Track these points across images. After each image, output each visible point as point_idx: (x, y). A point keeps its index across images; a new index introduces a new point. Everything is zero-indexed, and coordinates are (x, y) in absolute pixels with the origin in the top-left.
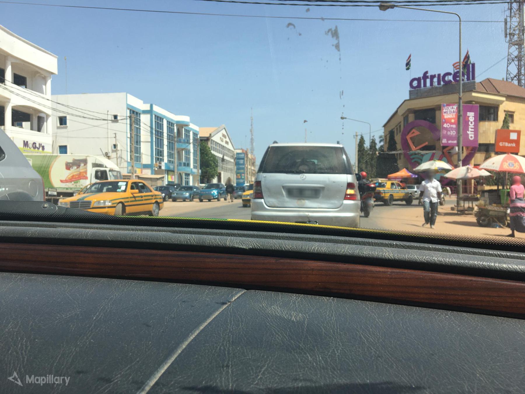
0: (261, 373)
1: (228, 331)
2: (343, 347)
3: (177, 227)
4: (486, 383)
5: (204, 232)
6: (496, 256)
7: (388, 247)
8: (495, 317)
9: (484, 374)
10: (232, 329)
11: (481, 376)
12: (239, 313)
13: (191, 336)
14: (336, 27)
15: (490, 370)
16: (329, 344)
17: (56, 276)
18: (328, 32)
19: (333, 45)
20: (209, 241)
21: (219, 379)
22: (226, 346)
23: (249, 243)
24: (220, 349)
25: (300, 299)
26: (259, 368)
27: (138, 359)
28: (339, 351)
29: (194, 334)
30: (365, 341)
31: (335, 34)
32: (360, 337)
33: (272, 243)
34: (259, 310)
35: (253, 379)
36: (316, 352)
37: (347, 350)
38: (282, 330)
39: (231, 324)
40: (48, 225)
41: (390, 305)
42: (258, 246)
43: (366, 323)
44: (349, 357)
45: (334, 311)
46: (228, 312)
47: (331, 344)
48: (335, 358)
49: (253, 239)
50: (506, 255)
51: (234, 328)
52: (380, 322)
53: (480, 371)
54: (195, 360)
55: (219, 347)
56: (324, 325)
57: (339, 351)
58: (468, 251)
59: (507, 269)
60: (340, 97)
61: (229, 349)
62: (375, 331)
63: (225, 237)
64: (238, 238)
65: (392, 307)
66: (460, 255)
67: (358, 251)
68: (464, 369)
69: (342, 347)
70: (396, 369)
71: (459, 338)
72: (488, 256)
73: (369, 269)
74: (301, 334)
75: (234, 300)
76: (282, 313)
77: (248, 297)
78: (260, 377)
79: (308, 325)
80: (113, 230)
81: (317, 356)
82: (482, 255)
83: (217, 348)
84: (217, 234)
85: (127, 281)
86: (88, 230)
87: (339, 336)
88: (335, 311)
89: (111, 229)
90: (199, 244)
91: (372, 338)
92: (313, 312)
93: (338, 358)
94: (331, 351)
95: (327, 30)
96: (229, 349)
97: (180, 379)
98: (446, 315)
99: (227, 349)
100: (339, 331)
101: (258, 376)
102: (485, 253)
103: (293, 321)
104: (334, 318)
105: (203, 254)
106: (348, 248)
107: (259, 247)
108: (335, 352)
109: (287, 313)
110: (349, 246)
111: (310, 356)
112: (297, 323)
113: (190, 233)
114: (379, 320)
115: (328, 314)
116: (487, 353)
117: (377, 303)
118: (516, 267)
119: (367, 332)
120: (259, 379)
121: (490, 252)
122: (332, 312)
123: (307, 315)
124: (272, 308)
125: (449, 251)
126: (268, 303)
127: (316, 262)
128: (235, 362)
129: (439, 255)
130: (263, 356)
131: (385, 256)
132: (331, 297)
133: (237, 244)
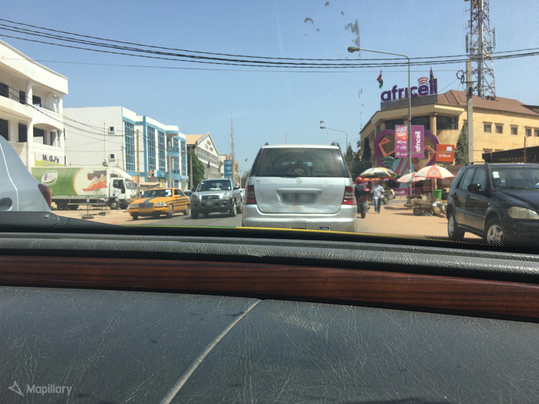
0: (284, 387)
1: (246, 343)
6: (520, 259)
7: (407, 252)
8: (523, 323)
10: (250, 340)
12: (256, 324)
13: (207, 349)
16: (353, 355)
20: (220, 249)
23: (262, 251)
24: (239, 362)
25: (319, 309)
26: (282, 382)
27: (153, 375)
28: (364, 362)
29: (210, 347)
30: (391, 350)
32: (386, 347)
35: (276, 393)
37: (372, 361)
38: (303, 341)
39: (248, 336)
41: (413, 312)
42: (272, 254)
45: (355, 320)
46: (244, 323)
47: (355, 354)
48: (360, 370)
49: (267, 246)
50: (530, 258)
51: (252, 340)
52: (405, 331)
54: (213, 375)
55: (237, 360)
57: (364, 362)
60: (359, 95)
63: (237, 245)
64: (250, 245)
65: (415, 315)
66: (483, 259)
67: (376, 257)
71: (488, 345)
72: (511, 259)
73: (388, 276)
74: (323, 345)
76: (301, 323)
77: (264, 307)
79: (329, 335)
81: (342, 368)
82: (505, 259)
83: (235, 361)
84: (227, 242)
85: (136, 292)
86: (92, 241)
88: (357, 320)
89: (116, 239)
91: (397, 347)
92: (333, 321)
93: (364, 369)
94: (355, 363)
97: (199, 396)
98: (473, 321)
100: (362, 342)
101: (281, 390)
102: (508, 257)
103: (313, 332)
104: (356, 327)
106: (366, 254)
107: (273, 254)
108: (359, 363)
109: (307, 324)
110: (367, 252)
112: (317, 333)
113: (200, 241)
114: (404, 328)
115: (349, 323)
117: (399, 311)
119: (392, 341)
120: (282, 394)
122: (354, 320)
124: (291, 318)
125: (471, 255)
126: (286, 313)
127: (332, 269)
128: (255, 376)
129: (461, 260)
130: (285, 369)
133: (249, 252)
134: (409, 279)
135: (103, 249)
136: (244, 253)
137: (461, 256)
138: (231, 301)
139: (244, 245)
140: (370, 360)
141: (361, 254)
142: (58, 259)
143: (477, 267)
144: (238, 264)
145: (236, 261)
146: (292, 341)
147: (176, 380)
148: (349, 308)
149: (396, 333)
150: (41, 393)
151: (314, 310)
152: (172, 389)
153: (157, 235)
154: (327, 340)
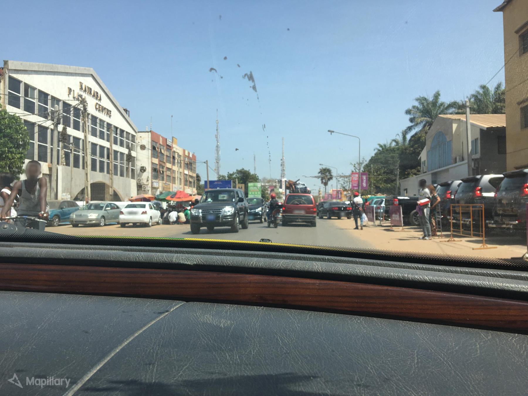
2: (259, 348)
3: (130, 246)
4: (374, 374)
9: (374, 367)
10: (164, 334)
11: (372, 369)
12: (173, 321)
14: (251, 72)
15: (380, 363)
19: (250, 87)
20: (156, 258)
21: (144, 376)
26: (182, 366)
28: (255, 351)
31: (251, 78)
32: (277, 339)
34: (193, 318)
37: (263, 350)
41: (312, 312)
42: (202, 262)
43: (286, 327)
44: (262, 356)
46: (163, 321)
48: (250, 357)
49: (198, 256)
51: (166, 334)
52: (299, 327)
55: (149, 350)
56: (248, 330)
57: (255, 351)
58: (389, 264)
59: (418, 279)
61: (157, 352)
66: (380, 268)
67: (291, 265)
68: (359, 363)
69: (259, 348)
70: (301, 364)
72: (407, 268)
75: (172, 310)
76: (213, 321)
79: (233, 330)
80: (68, 248)
82: (402, 268)
83: (147, 350)
87: (258, 339)
89: (65, 248)
90: (147, 261)
91: (287, 340)
95: (244, 75)
96: (157, 352)
97: (109, 378)
98: (359, 319)
101: (180, 373)
105: (150, 270)
106: (283, 263)
107: (203, 263)
109: (217, 321)
111: (229, 356)
116: (382, 350)
117: (301, 311)
118: (426, 277)
119: (285, 335)
120: (179, 376)
121: (409, 265)
123: (235, 322)
124: (205, 317)
128: (161, 362)
130: (187, 357)
131: (314, 269)
134: (317, 284)
135: (50, 256)
136: (177, 261)
137: (365, 265)
139: (179, 254)
141: (279, 262)
143: (373, 274)
144: (172, 271)
146: (200, 335)
147: (93, 366)
149: (291, 329)
151: (228, 311)
152: (89, 372)
153: (104, 245)
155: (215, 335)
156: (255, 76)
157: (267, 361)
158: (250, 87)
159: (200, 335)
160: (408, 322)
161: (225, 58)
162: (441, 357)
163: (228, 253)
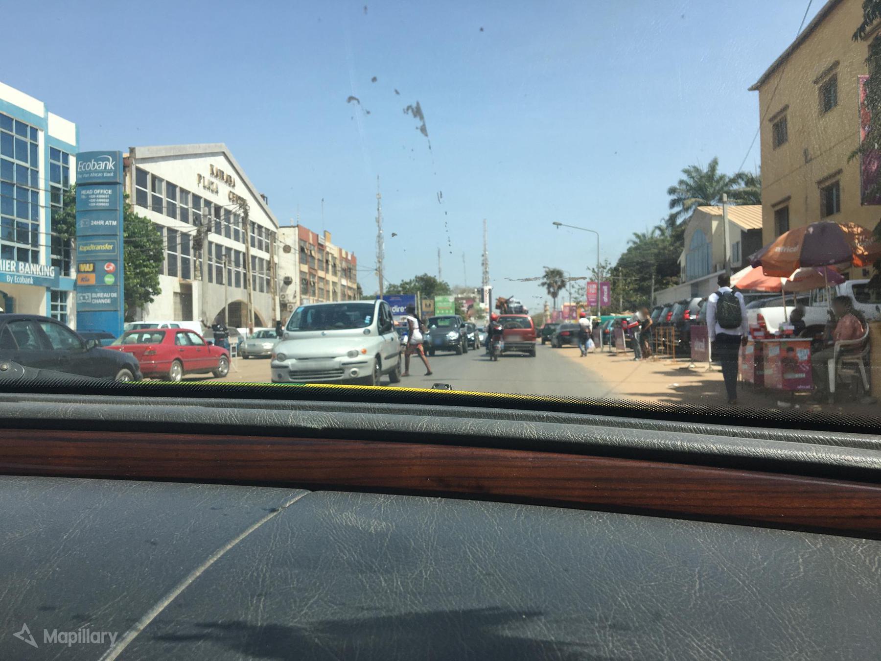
2: (435, 567)
5: (256, 405)
10: (276, 546)
11: (623, 599)
14: (418, 104)
15: (639, 591)
17: (13, 477)
18: (408, 109)
21: (244, 616)
22: (262, 570)
24: (252, 575)
31: (417, 112)
32: (465, 552)
33: (358, 419)
36: (394, 574)
37: (441, 571)
40: (4, 398)
41: (523, 505)
42: (337, 423)
44: (441, 581)
48: (420, 583)
49: (330, 413)
50: (706, 429)
51: (278, 546)
52: (500, 531)
53: (624, 593)
59: (699, 450)
60: (439, 200)
61: (264, 575)
62: (488, 542)
63: (287, 412)
66: (634, 430)
68: (602, 591)
70: (505, 594)
75: (288, 505)
76: (357, 522)
78: (304, 612)
81: (395, 580)
82: (671, 431)
83: (247, 574)
86: (68, 405)
89: (106, 402)
90: (245, 424)
94: (416, 573)
95: (406, 107)
96: (264, 575)
99: (262, 576)
101: (302, 610)
105: (251, 438)
107: (338, 425)
108: (422, 573)
109: (364, 522)
111: (385, 580)
113: (234, 406)
116: (641, 569)
117: (504, 504)
118: (712, 446)
120: (302, 615)
123: (394, 524)
130: (315, 583)
132: (437, 497)
136: (295, 423)
138: (265, 493)
139: (298, 411)
140: (438, 570)
142: (14, 433)
145: (265, 435)
146: (336, 546)
148: (434, 501)
150: (66, 642)
154: (386, 545)
155: (361, 546)
156: (425, 111)
157: (449, 589)
158: (417, 128)
159: (336, 546)
160: (682, 520)
161: (374, 79)
162: (739, 579)
163: (380, 409)
